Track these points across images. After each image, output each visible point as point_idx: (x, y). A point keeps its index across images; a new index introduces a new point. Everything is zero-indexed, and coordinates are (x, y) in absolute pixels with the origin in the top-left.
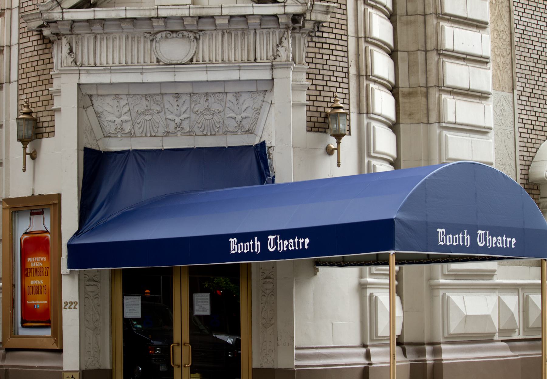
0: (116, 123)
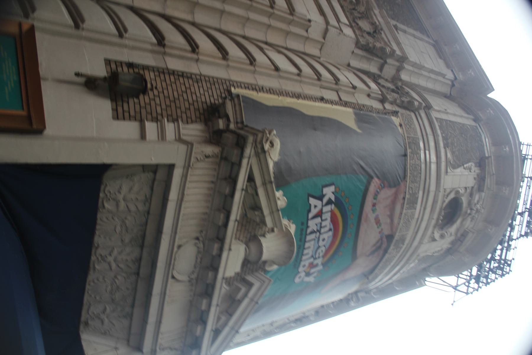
0: (117, 193)
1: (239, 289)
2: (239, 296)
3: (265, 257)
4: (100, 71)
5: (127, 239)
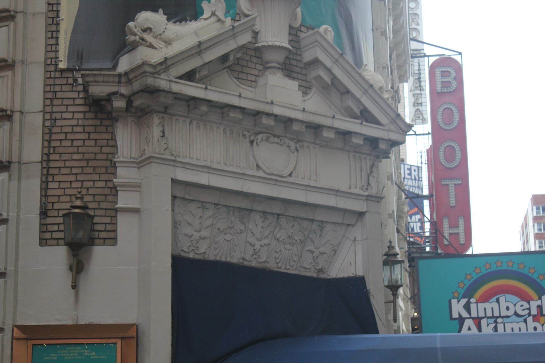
0: (192, 239)
1: (319, 78)
2: (327, 79)
3: (286, 45)
4: (60, 255)
5: (239, 226)
